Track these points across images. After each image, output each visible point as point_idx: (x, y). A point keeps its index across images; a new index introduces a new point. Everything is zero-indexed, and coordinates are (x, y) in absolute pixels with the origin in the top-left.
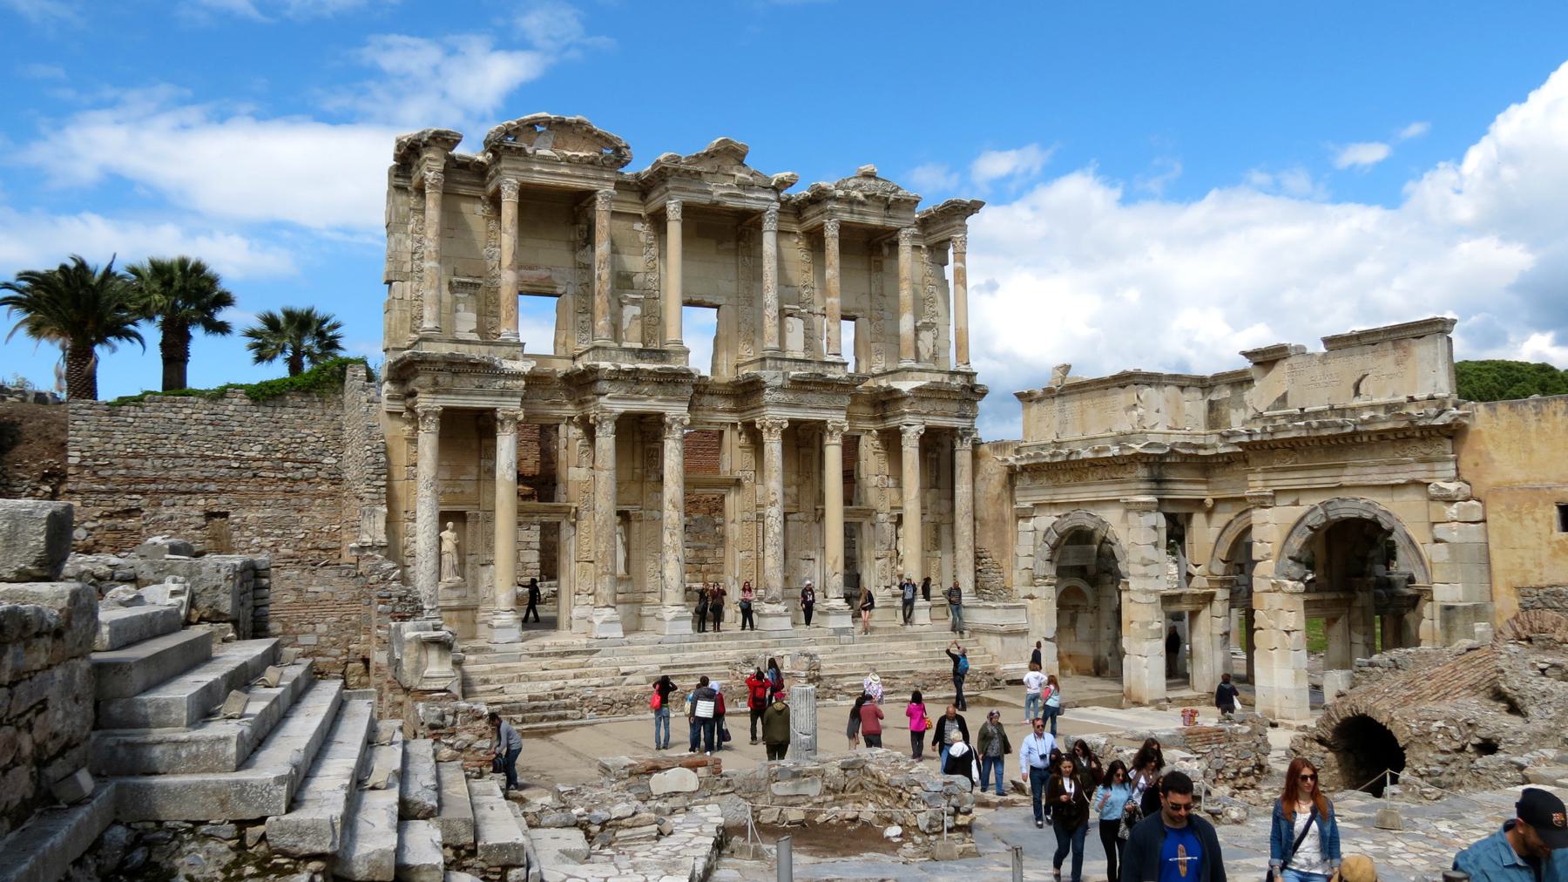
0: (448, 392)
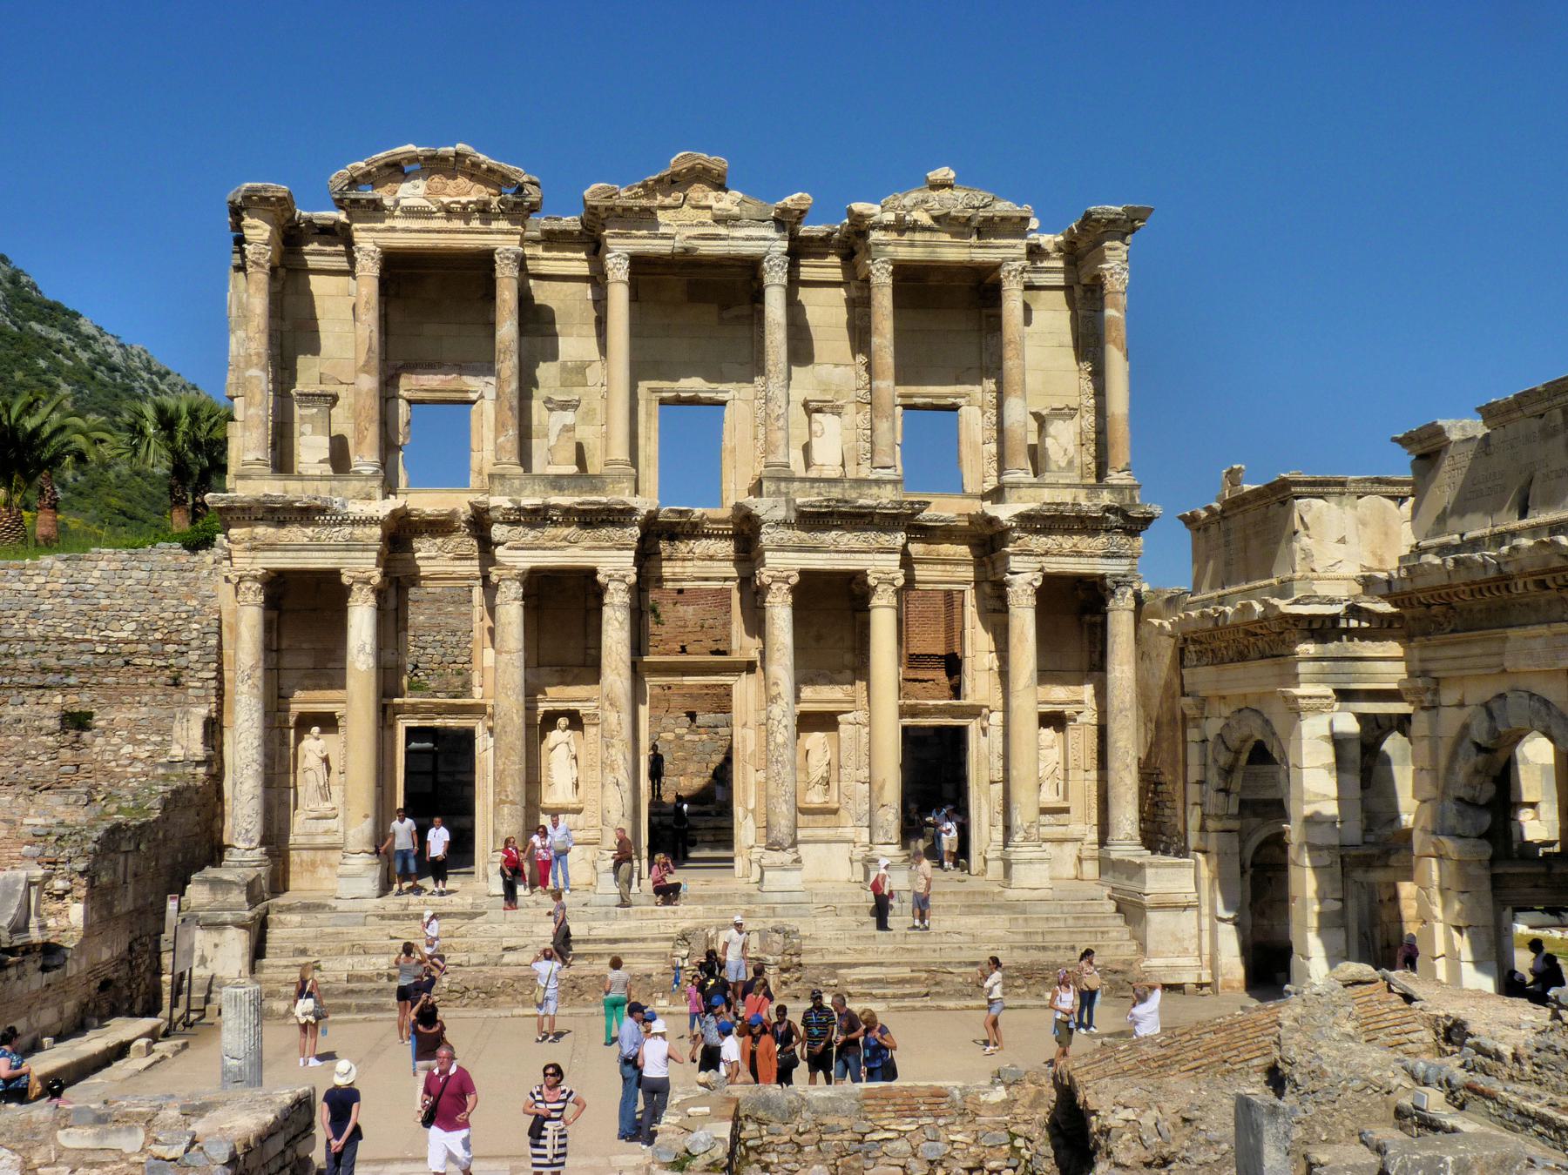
0: (272, 547)
